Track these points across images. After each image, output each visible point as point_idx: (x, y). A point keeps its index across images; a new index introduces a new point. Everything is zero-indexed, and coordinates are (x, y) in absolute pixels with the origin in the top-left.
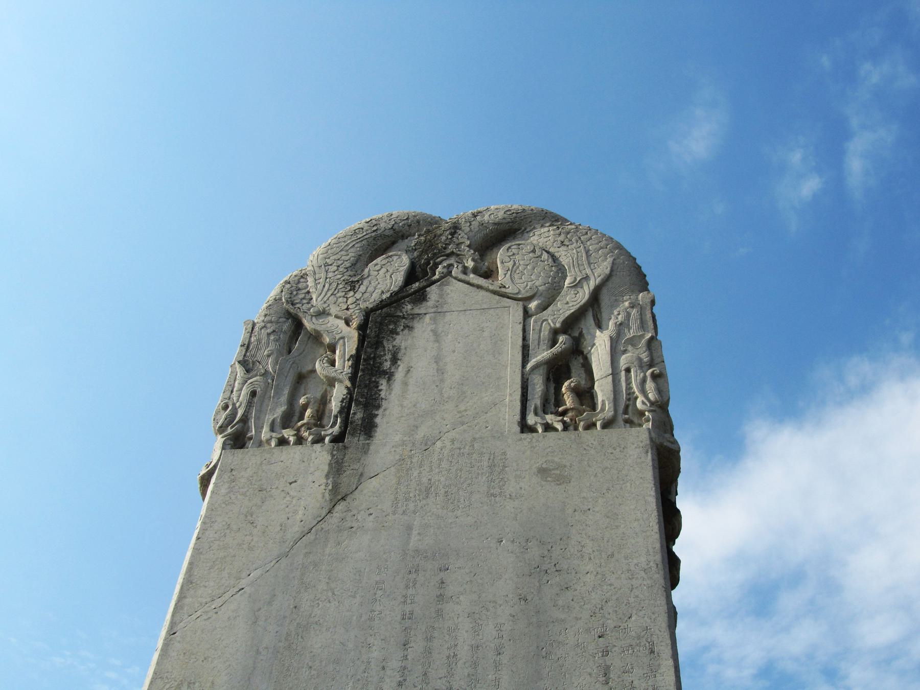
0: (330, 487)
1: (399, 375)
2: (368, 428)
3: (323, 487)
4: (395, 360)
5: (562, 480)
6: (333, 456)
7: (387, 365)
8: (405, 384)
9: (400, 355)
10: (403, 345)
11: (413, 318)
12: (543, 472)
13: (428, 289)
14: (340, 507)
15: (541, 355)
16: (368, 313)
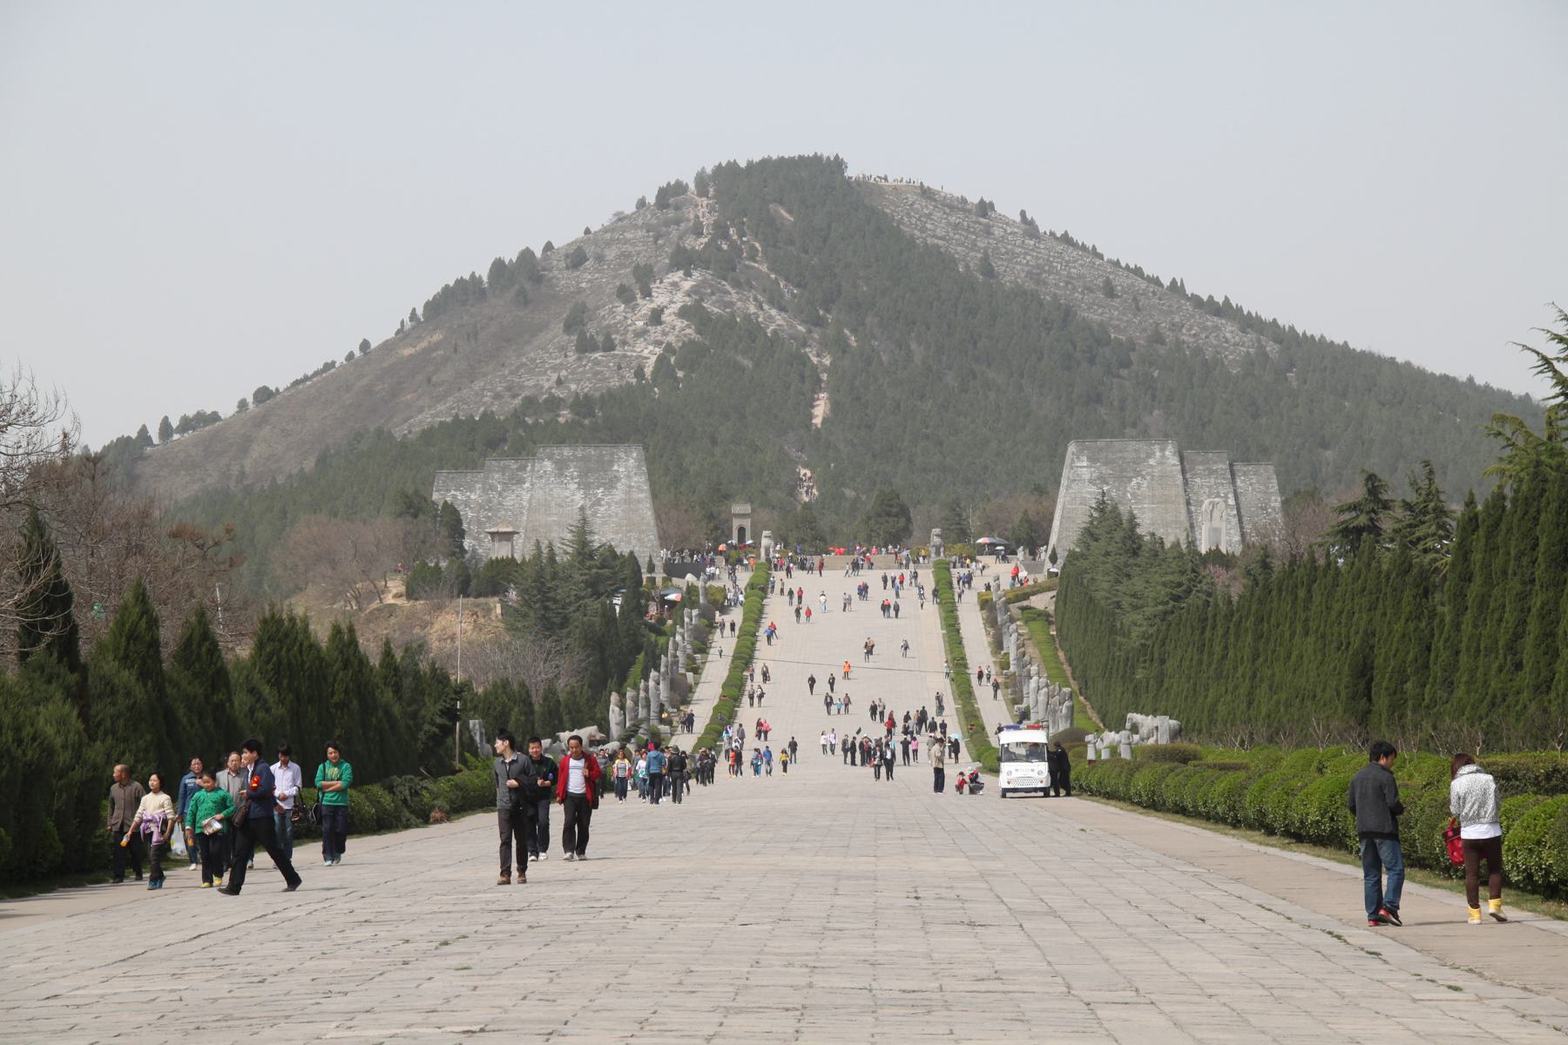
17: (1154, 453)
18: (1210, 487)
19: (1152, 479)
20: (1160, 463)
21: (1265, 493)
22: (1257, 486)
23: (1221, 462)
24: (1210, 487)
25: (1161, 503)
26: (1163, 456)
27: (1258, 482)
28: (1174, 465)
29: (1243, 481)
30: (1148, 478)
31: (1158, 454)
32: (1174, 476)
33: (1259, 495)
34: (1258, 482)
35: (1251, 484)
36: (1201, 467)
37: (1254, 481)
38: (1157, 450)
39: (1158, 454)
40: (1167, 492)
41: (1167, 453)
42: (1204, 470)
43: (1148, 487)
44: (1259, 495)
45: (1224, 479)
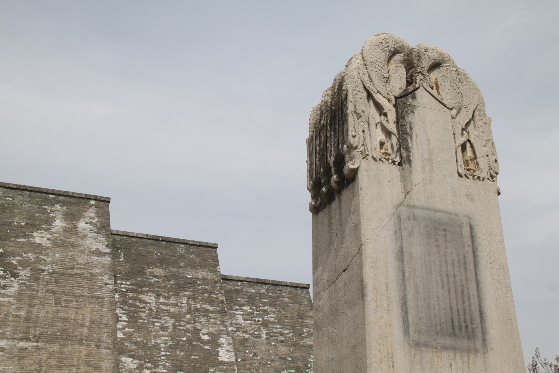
0: (403, 187)
1: (414, 137)
2: (409, 161)
3: (400, 186)
4: (411, 129)
5: (473, 200)
6: (401, 172)
7: (408, 130)
8: (417, 142)
9: (412, 126)
10: (413, 121)
11: (413, 107)
12: (467, 196)
13: (416, 92)
14: (408, 196)
15: (461, 140)
16: (396, 98)
17: (49, 221)
18: (177, 317)
19: (36, 277)
20: (58, 244)
21: (295, 345)
22: (278, 328)
23: (203, 267)
24: (177, 317)
25: (50, 339)
26: (72, 231)
27: (280, 320)
28: (98, 253)
29: (248, 316)
30: (25, 273)
31: (59, 224)
32: (92, 278)
33: (283, 350)
34: (280, 320)
35: (265, 324)
36: (158, 271)
37: (271, 317)
38: (59, 215)
39: (59, 224)
40: (71, 314)
41: (82, 225)
42: (166, 278)
43: (19, 296)
44: (283, 350)
45: (211, 302)
